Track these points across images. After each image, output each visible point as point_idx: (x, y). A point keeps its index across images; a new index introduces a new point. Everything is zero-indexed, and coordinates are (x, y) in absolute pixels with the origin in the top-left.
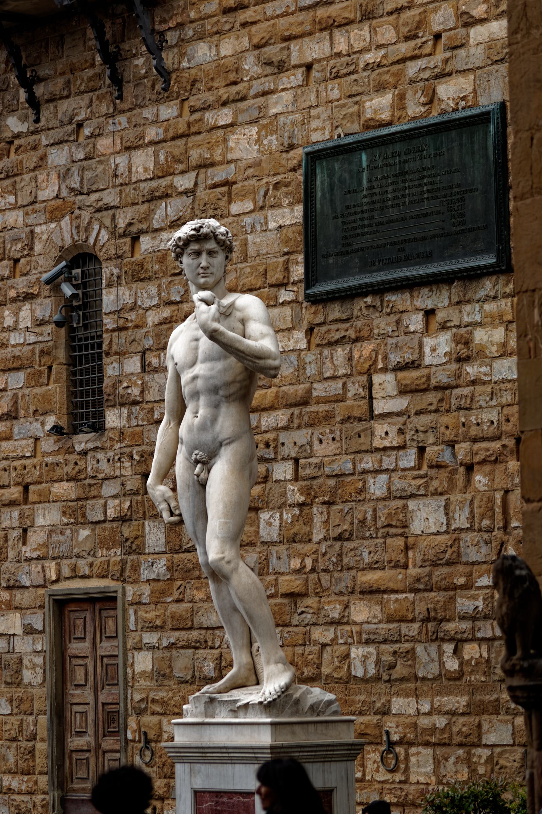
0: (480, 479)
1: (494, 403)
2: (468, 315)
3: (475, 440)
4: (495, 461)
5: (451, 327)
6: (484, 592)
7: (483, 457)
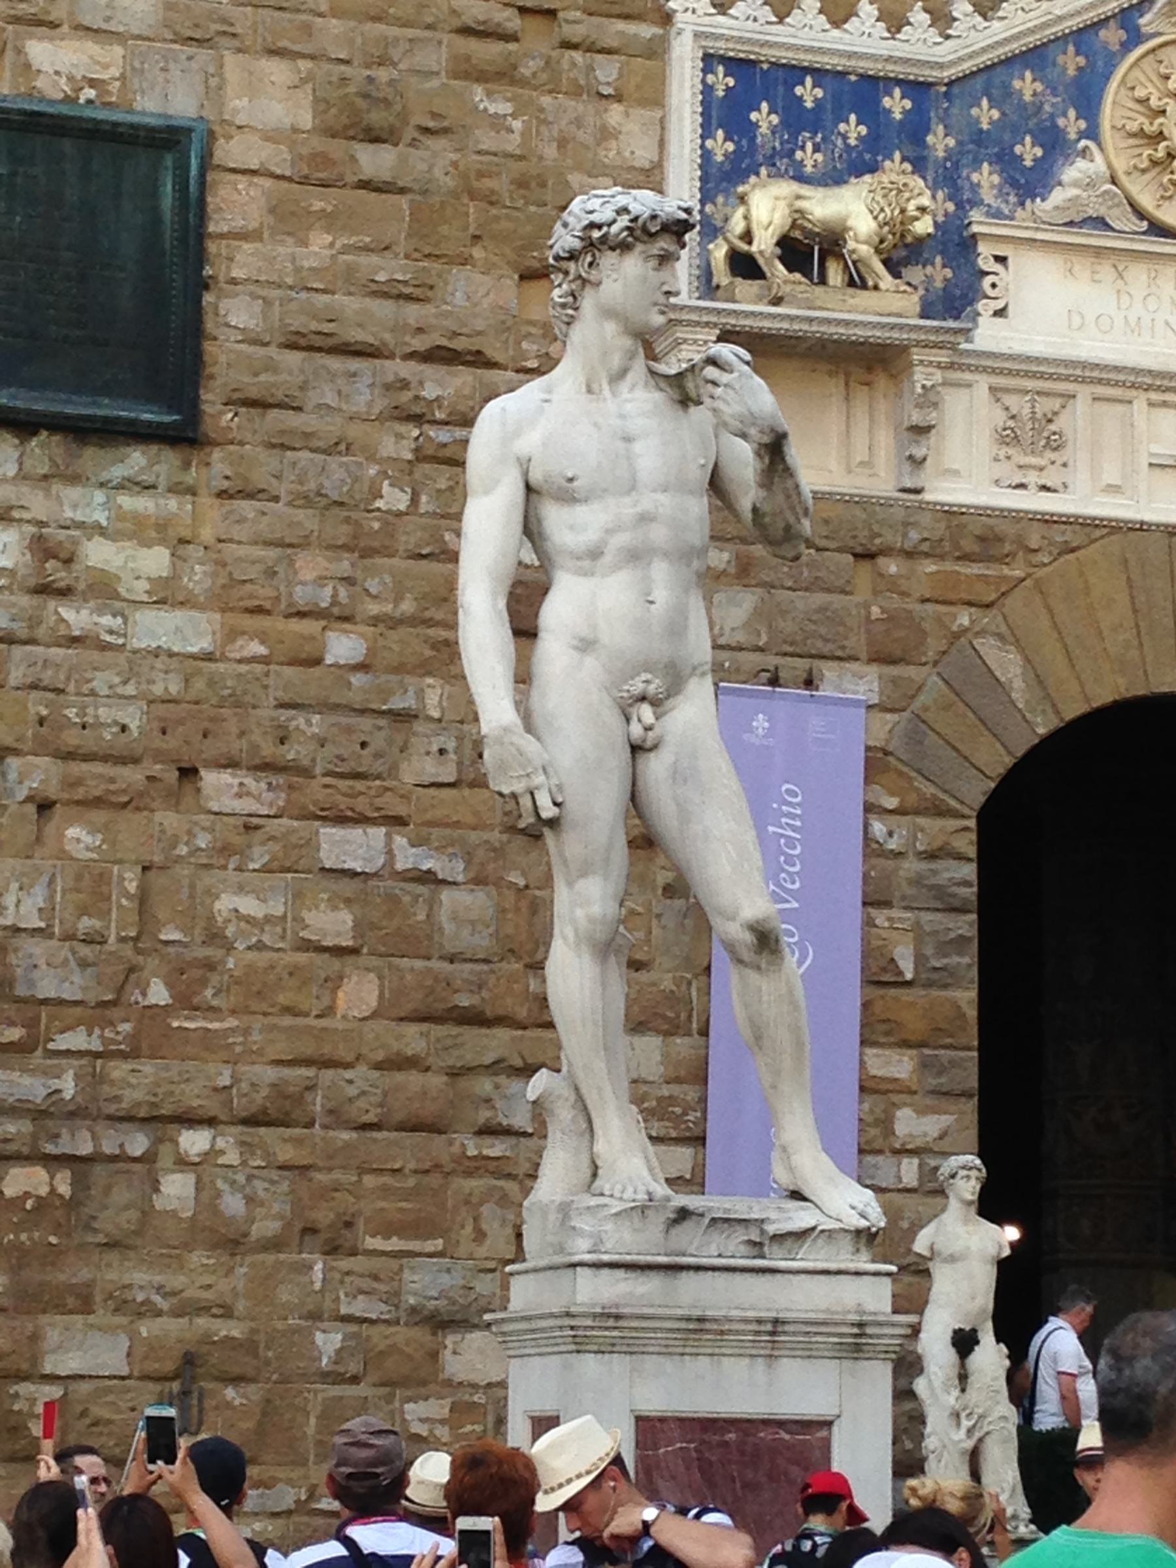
0: (79, 837)
1: (130, 690)
2: (75, 507)
3: (70, 756)
4: (125, 805)
5: (20, 520)
6: (76, 1063)
7: (97, 793)
